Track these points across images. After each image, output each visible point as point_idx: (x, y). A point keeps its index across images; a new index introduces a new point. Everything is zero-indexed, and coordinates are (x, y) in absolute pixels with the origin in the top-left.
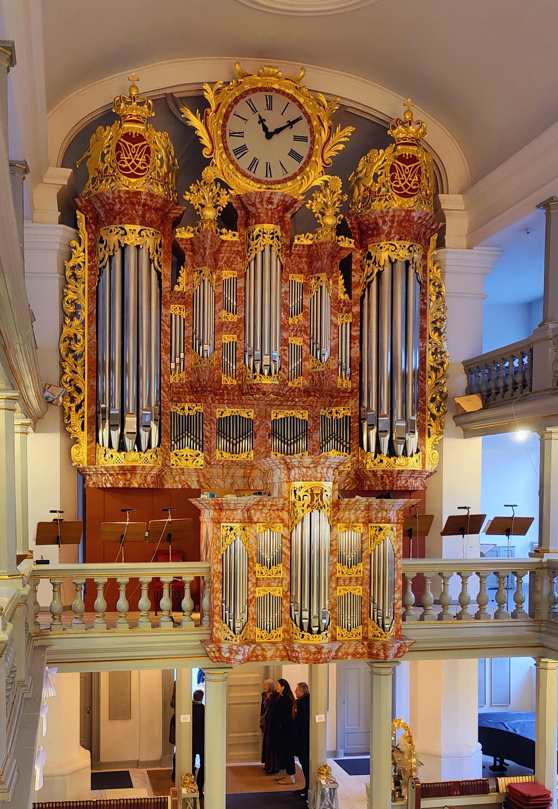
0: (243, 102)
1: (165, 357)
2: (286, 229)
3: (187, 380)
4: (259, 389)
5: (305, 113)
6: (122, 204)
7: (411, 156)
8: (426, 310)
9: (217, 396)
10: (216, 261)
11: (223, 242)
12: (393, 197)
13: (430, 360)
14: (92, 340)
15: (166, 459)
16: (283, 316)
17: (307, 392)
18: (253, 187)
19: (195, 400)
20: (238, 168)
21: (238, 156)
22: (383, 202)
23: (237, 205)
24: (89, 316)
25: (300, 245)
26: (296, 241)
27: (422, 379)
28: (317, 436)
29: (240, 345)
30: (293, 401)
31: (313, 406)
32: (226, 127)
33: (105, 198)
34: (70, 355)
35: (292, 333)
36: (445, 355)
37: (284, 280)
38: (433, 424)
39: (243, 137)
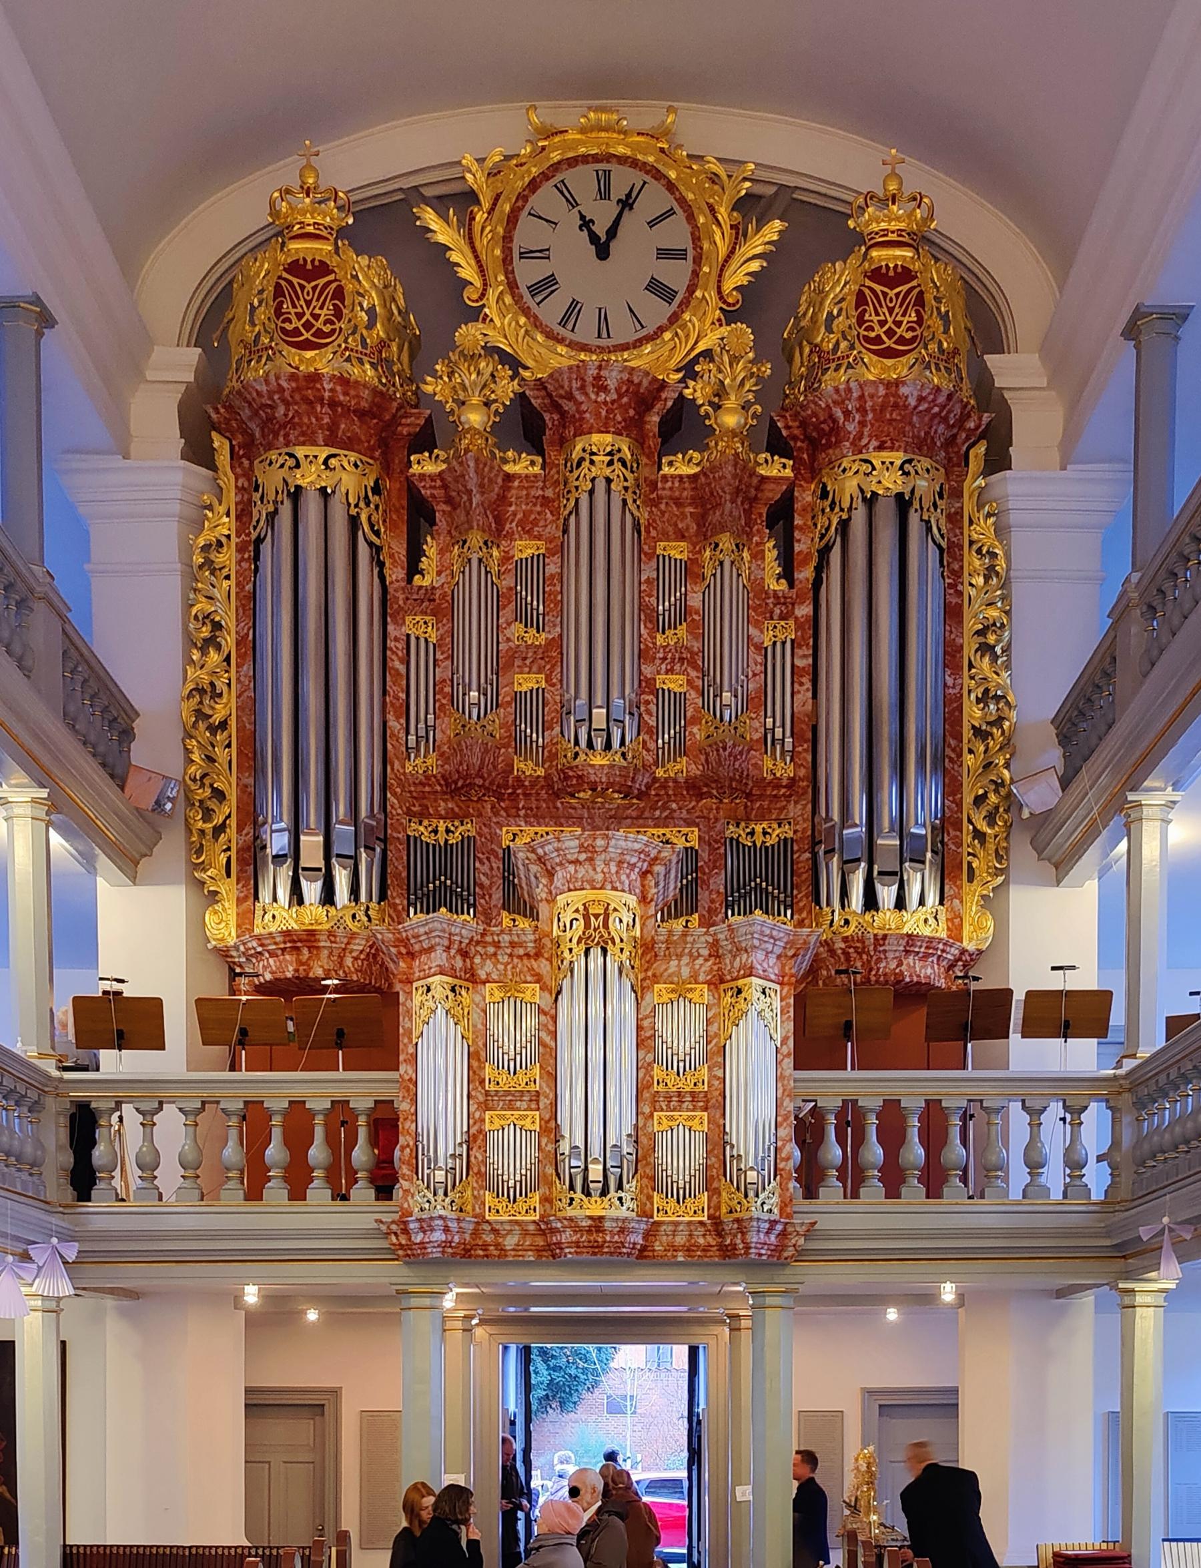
0: (547, 188)
1: (395, 724)
2: (650, 447)
3: (440, 769)
4: (580, 777)
5: (682, 201)
6: (287, 404)
7: (899, 270)
8: (961, 606)
9: (503, 800)
10: (500, 521)
11: (509, 477)
12: (862, 359)
13: (973, 714)
14: (246, 694)
16: (643, 631)
17: (694, 788)
19: (456, 809)
20: (536, 323)
21: (538, 299)
22: (842, 371)
23: (539, 401)
24: (238, 644)
25: (672, 476)
26: (666, 470)
27: (953, 755)
29: (552, 696)
30: (664, 807)
31: (709, 820)
32: (512, 241)
33: (255, 394)
34: (202, 726)
35: (663, 666)
36: (1008, 703)
38: (981, 854)
39: (548, 258)
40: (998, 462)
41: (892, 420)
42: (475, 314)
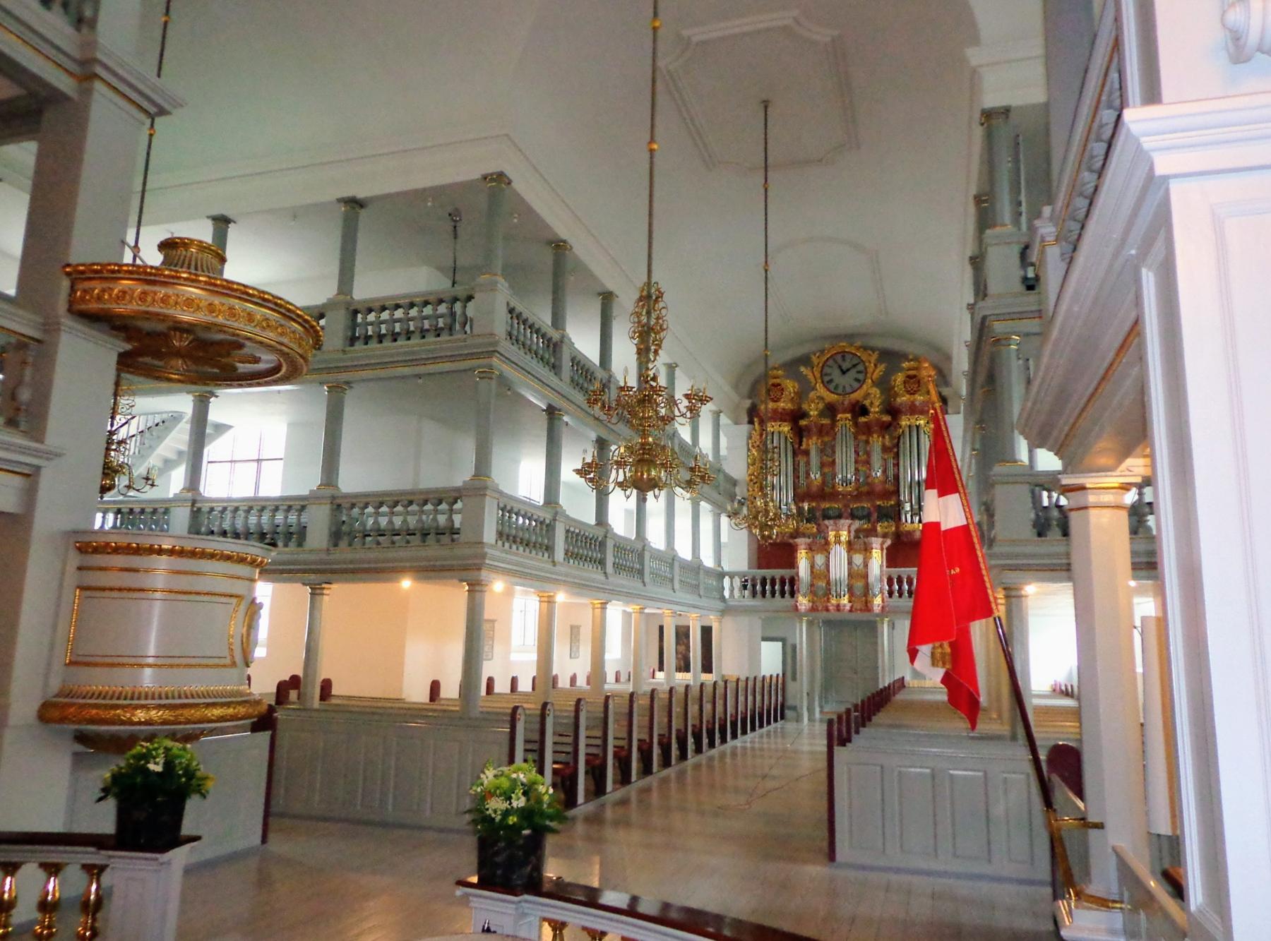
37: (856, 438)
42: (814, 389)
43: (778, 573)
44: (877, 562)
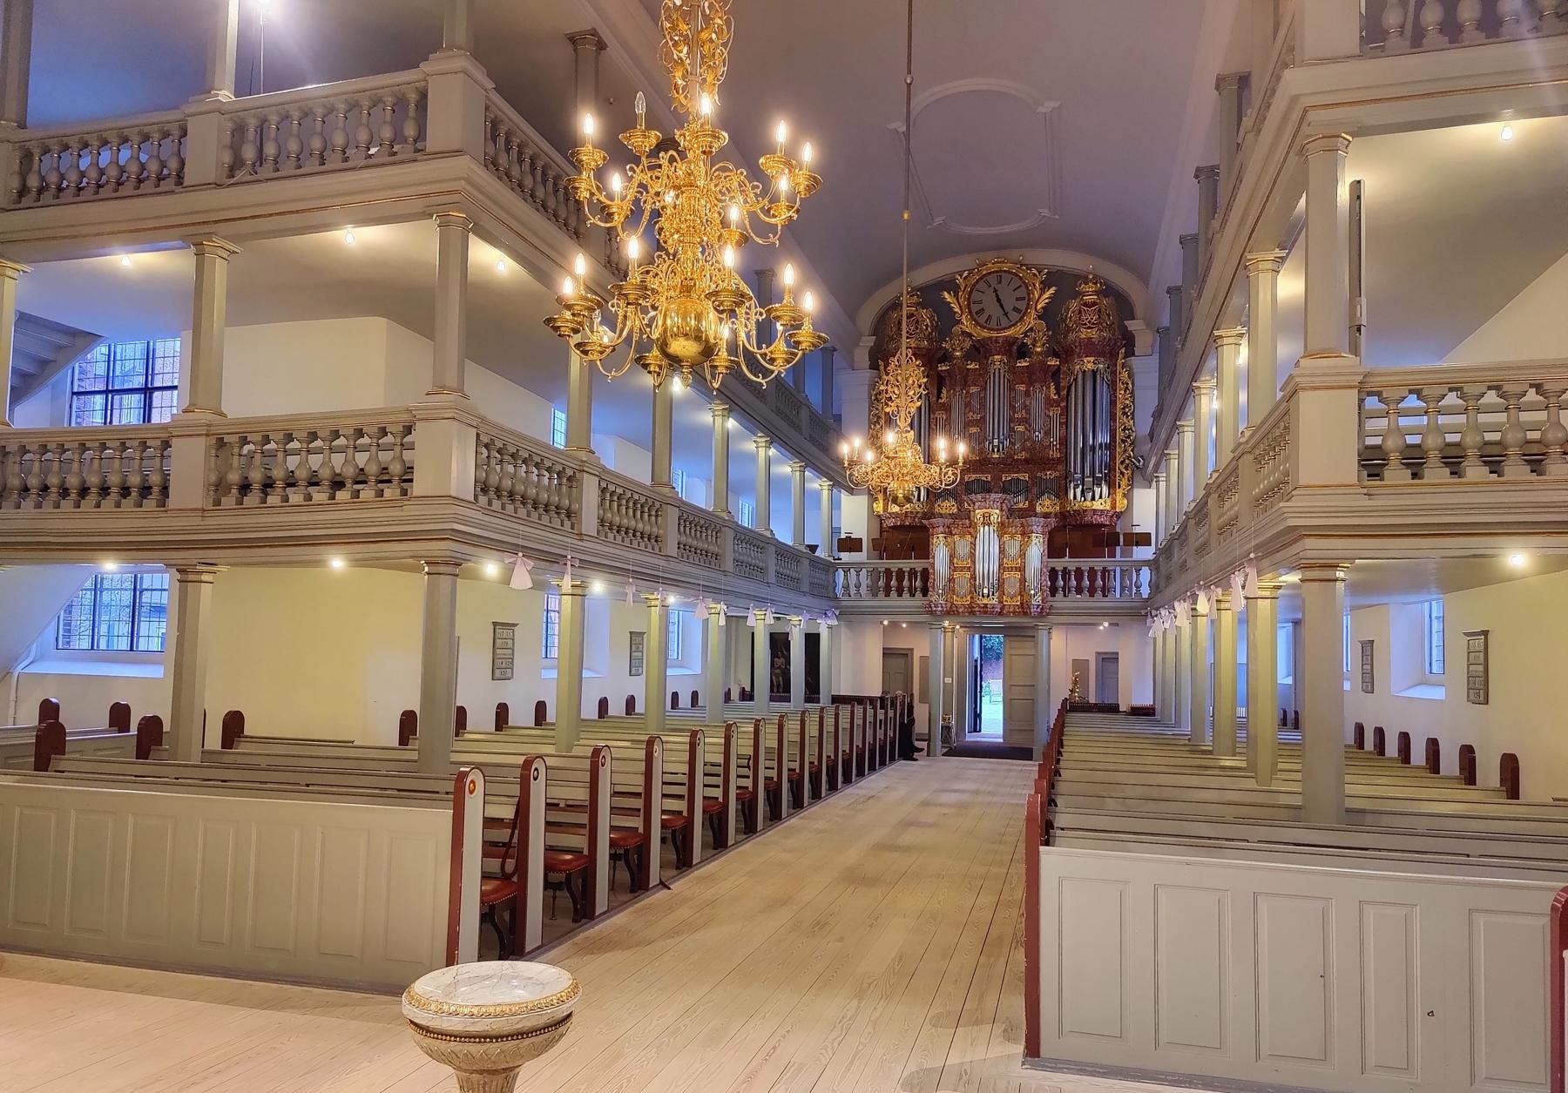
15: (932, 507)
18: (985, 334)
28: (1034, 490)
37: (1011, 389)
40: (1130, 353)
41: (1090, 348)
43: (906, 565)
44: (1036, 550)
